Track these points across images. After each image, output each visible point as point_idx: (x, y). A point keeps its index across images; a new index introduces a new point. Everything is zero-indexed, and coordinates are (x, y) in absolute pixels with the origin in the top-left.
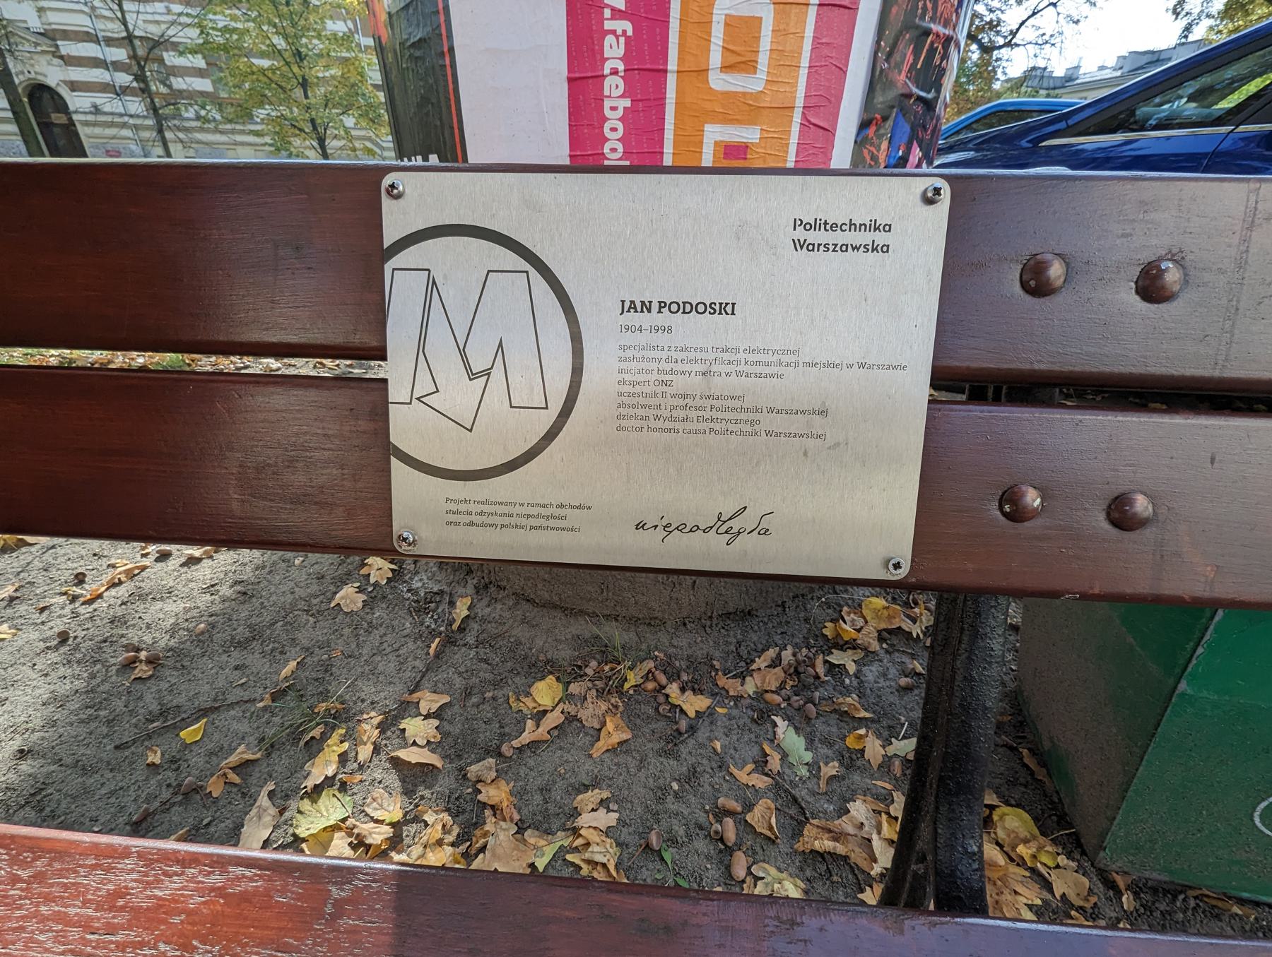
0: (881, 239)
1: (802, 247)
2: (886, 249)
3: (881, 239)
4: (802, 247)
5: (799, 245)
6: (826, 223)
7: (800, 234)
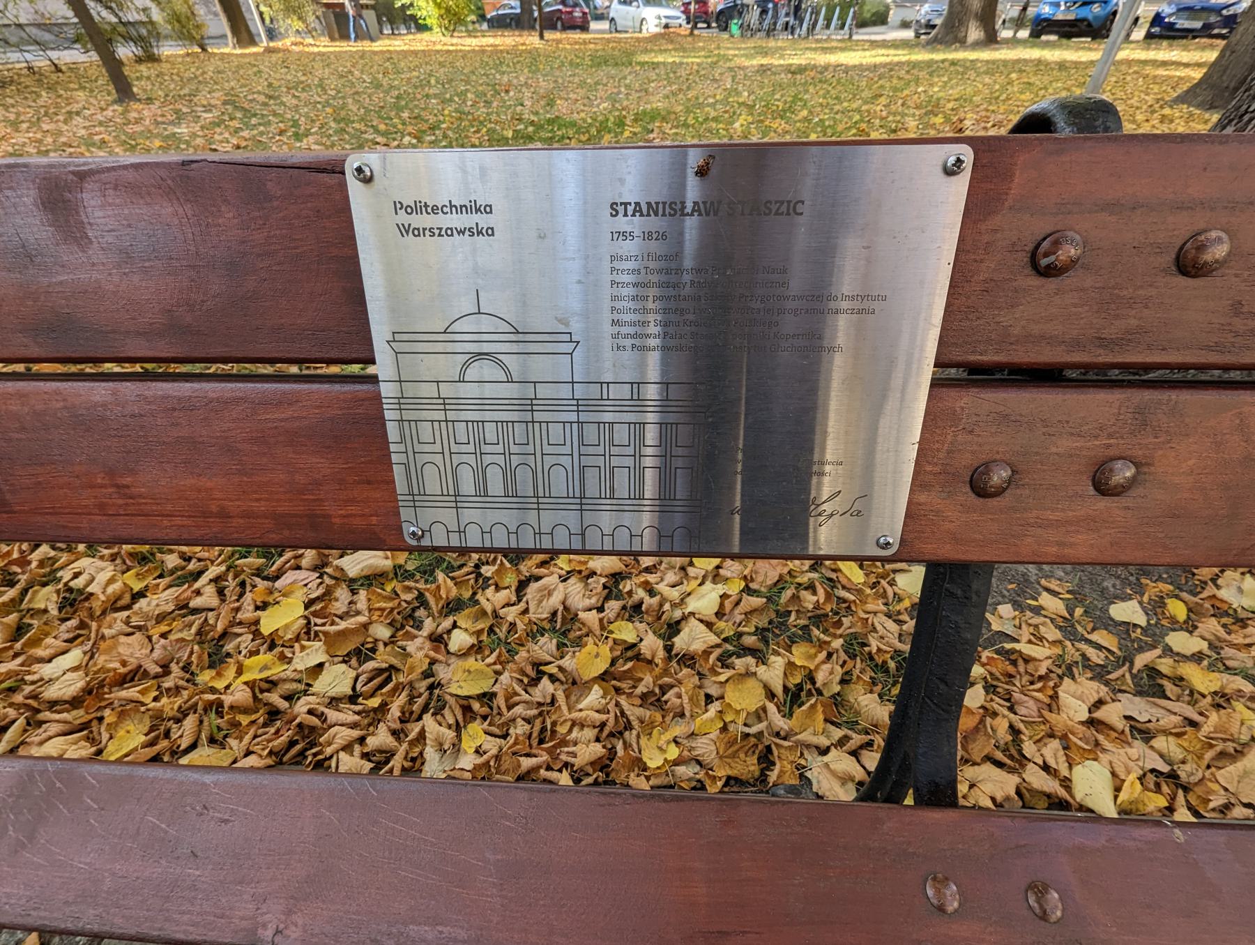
0: (483, 220)
1: (407, 232)
2: (491, 232)
3: (483, 220)
4: (407, 232)
5: (405, 230)
6: (426, 206)
7: (403, 218)
